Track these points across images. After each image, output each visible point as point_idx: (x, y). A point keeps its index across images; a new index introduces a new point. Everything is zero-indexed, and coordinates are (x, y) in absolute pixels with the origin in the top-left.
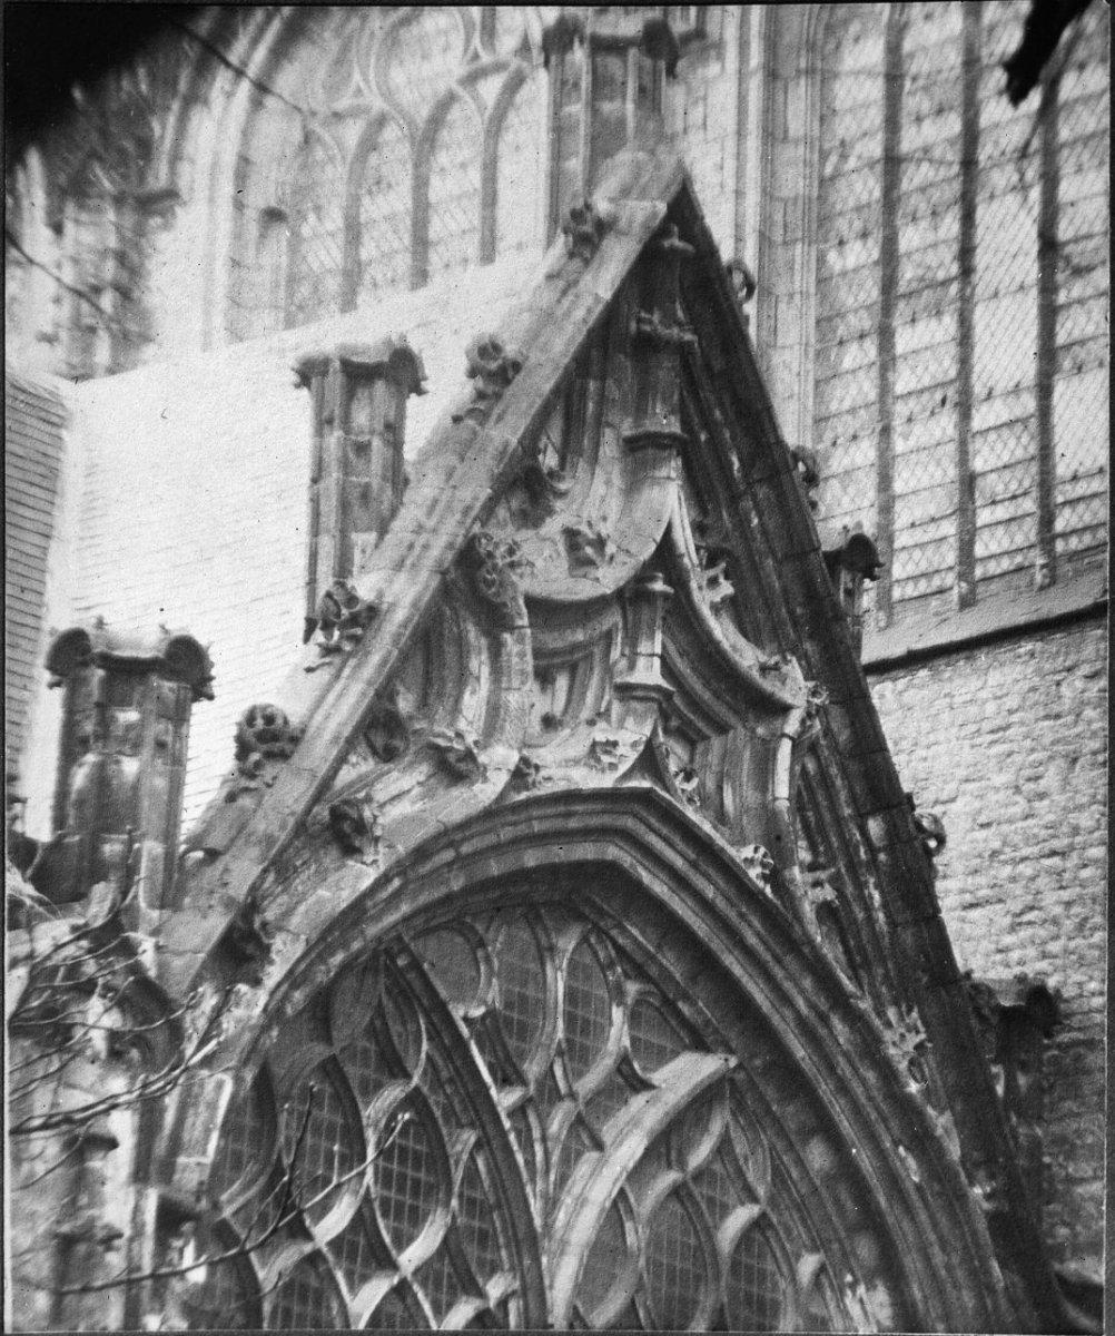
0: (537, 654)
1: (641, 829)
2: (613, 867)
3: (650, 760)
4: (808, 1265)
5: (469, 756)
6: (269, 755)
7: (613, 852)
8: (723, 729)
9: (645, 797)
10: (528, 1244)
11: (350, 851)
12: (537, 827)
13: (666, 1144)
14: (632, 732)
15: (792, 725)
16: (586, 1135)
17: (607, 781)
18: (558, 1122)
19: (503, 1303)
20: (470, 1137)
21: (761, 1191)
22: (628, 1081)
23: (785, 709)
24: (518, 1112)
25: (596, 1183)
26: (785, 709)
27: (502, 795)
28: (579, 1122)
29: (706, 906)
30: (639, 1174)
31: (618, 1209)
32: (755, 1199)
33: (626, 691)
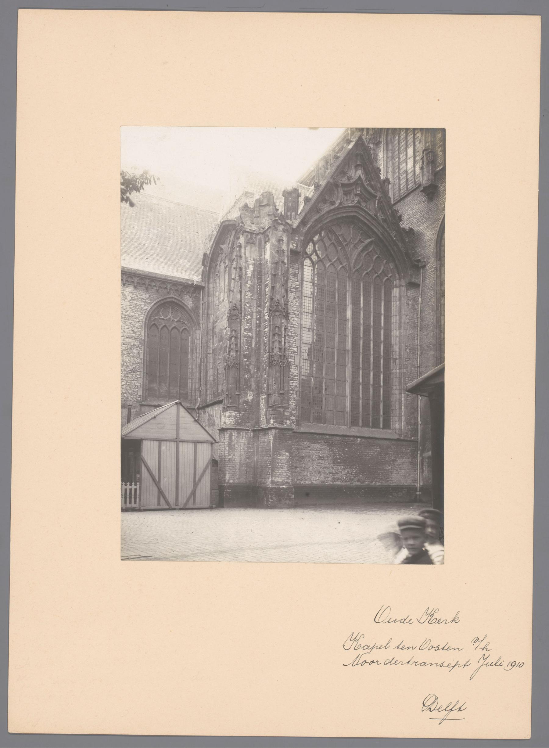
0: (344, 191)
1: (358, 211)
2: (355, 216)
3: (359, 202)
4: (385, 261)
5: (334, 202)
6: (307, 202)
7: (355, 214)
8: (369, 200)
9: (358, 207)
10: (348, 259)
11: (319, 213)
12: (345, 211)
13: (365, 248)
14: (356, 199)
15: (377, 198)
16: (355, 247)
17: (353, 205)
18: (352, 245)
19: (346, 265)
20: (340, 248)
21: (378, 253)
22: (361, 241)
23: (376, 196)
24: (346, 245)
25: (356, 252)
26: (376, 196)
27: (338, 206)
28: (354, 246)
29: (368, 220)
30: (362, 251)
31: (359, 255)
32: (377, 254)
33: (356, 195)
